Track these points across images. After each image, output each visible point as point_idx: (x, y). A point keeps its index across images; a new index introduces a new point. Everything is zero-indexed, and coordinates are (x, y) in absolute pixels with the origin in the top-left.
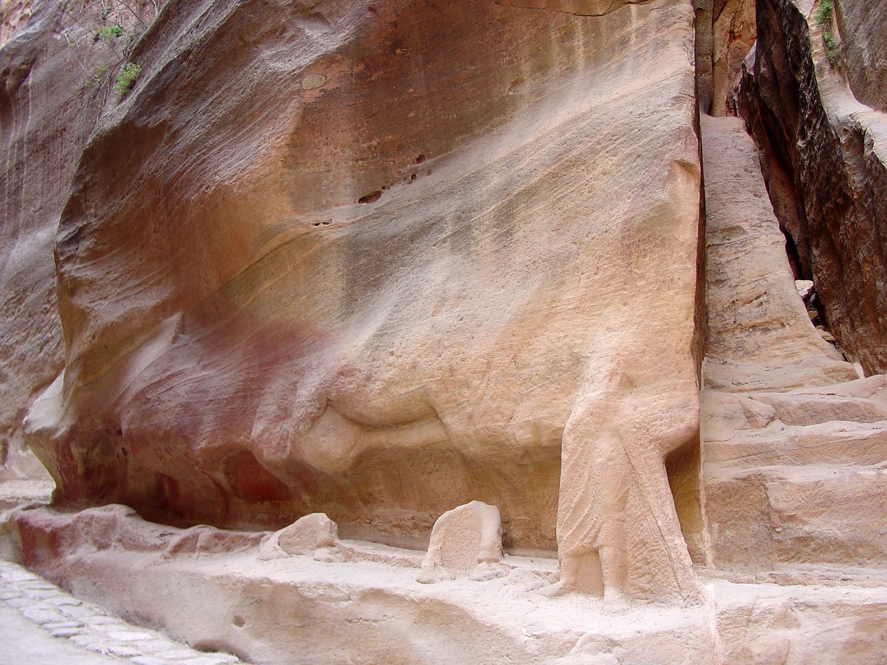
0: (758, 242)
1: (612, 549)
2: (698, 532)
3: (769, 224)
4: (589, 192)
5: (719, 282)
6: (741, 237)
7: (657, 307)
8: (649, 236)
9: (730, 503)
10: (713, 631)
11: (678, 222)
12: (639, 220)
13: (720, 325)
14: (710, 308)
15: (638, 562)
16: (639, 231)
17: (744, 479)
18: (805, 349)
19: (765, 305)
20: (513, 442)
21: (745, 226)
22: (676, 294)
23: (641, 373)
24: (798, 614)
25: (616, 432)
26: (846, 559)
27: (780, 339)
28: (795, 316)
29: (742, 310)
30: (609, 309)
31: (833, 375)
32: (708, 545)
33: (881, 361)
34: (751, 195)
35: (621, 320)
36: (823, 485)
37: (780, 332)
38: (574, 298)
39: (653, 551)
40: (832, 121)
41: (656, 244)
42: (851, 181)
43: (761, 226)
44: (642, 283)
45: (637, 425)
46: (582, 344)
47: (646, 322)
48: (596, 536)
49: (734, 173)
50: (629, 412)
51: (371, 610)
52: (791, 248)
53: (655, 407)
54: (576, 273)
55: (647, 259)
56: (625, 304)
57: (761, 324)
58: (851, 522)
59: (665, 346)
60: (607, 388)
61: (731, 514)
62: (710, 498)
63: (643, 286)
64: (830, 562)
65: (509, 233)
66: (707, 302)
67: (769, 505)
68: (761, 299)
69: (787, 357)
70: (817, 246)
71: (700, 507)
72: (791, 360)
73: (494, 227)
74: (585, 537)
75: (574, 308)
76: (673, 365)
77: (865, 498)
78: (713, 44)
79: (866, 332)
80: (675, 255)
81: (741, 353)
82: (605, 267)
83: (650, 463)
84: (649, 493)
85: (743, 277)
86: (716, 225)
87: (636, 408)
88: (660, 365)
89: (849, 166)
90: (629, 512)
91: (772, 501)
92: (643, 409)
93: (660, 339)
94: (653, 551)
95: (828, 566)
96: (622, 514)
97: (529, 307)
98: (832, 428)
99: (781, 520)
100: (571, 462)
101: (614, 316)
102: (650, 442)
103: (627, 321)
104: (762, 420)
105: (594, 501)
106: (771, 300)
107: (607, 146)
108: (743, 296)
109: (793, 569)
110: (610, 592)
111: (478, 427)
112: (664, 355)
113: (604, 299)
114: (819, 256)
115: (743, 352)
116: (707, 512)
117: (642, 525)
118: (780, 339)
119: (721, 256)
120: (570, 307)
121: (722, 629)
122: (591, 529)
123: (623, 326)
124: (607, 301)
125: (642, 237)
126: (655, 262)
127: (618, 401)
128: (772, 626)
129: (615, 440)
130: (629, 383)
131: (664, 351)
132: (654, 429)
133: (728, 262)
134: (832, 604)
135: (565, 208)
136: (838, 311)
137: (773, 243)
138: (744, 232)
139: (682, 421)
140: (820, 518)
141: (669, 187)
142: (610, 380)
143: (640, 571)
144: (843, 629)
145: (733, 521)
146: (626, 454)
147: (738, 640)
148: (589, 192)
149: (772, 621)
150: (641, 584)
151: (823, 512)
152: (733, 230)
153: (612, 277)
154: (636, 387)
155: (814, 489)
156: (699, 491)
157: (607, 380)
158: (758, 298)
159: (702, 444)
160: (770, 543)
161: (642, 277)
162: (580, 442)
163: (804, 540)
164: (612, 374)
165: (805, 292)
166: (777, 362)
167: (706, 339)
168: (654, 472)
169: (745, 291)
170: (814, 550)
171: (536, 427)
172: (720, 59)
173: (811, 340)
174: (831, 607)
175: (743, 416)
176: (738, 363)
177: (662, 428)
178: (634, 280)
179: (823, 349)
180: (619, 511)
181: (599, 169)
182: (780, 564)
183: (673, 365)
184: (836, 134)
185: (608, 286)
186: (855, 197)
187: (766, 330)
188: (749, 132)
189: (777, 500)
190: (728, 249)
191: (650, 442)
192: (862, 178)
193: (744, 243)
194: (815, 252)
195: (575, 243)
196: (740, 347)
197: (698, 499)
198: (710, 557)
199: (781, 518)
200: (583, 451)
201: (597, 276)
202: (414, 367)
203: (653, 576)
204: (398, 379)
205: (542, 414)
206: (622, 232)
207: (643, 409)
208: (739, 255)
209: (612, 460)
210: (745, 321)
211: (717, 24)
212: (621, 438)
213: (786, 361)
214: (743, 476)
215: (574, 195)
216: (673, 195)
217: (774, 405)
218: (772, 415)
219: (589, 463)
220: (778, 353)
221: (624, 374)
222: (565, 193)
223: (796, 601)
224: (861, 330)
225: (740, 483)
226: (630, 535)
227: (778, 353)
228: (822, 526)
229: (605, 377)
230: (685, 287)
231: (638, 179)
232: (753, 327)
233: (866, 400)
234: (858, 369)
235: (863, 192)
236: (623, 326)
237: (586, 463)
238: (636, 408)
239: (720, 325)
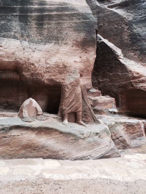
20: (43, 83)
51: (14, 133)
59: (89, 69)
65: (42, 24)
73: (36, 20)
74: (73, 109)
97: (51, 48)
100: (70, 92)
105: (77, 101)
107: (77, 16)
111: (34, 77)
171: (52, 80)
191: (86, 89)
202: (13, 54)
203: (87, 118)
204: (5, 56)
205: (53, 77)
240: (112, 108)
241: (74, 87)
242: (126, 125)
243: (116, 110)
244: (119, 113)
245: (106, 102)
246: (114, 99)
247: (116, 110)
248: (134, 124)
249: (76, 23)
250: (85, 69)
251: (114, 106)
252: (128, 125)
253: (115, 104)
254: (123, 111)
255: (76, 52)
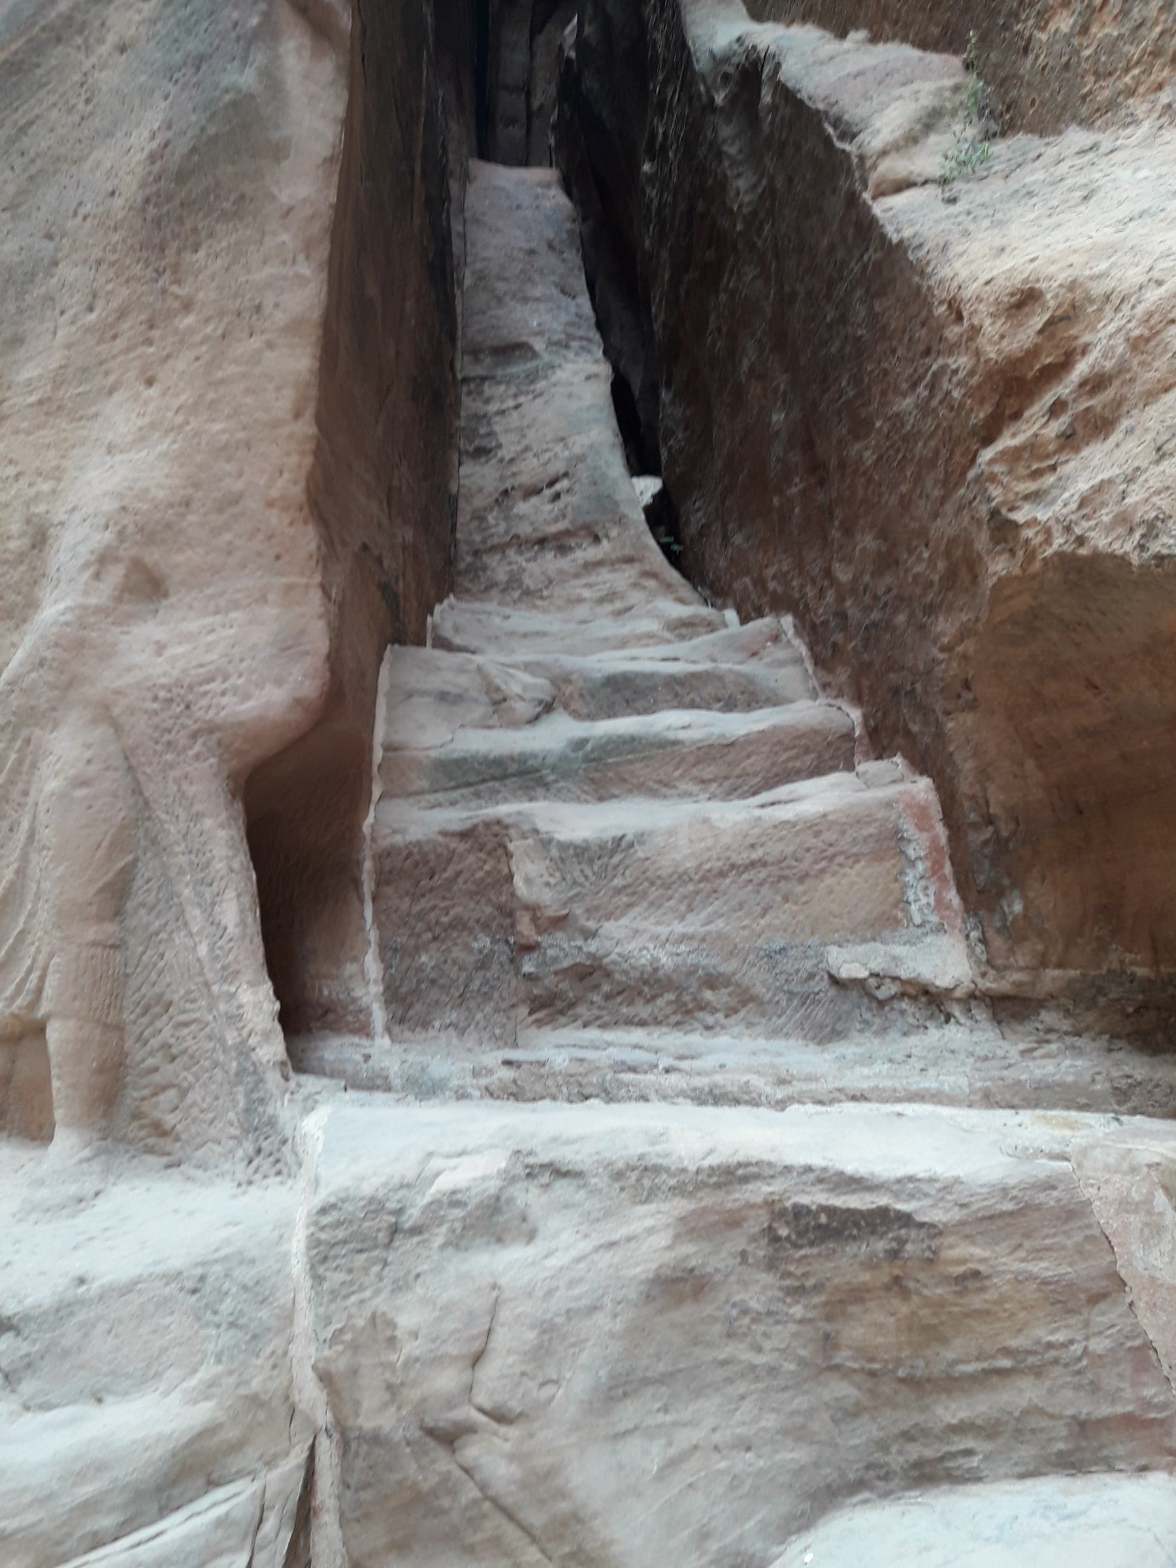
0: (560, 375)
1: (72, 1023)
2: (355, 959)
3: (584, 343)
4: (88, 101)
5: (482, 453)
6: (529, 365)
7: (222, 382)
8: (207, 192)
9: (431, 890)
10: (298, 1266)
11: (278, 152)
12: (182, 146)
13: (477, 538)
14: (462, 504)
15: (151, 1054)
16: (181, 177)
17: (464, 835)
18: (635, 585)
19: (565, 499)
21: (538, 345)
22: (270, 345)
23: (180, 558)
24: (529, 1197)
25: (104, 713)
26: (678, 1017)
27: (590, 566)
28: (621, 521)
29: (522, 507)
30: (117, 397)
31: (683, 628)
32: (376, 989)
33: (774, 594)
34: (555, 292)
35: (140, 422)
36: (631, 845)
37: (591, 553)
38: (41, 377)
39: (186, 1024)
40: (702, 64)
41: (224, 212)
42: (732, 193)
43: (567, 347)
44: (189, 320)
45: (162, 694)
46: (54, 492)
47: (194, 423)
48: (39, 990)
49: (526, 246)
50: (139, 658)
52: (620, 392)
53: (209, 648)
54: (49, 313)
55: (202, 253)
56: (150, 382)
57: (558, 536)
58: (690, 930)
59: (239, 486)
60: (86, 593)
61: (432, 916)
62: (383, 878)
63: (191, 331)
64: (642, 1024)
66: (454, 489)
67: (513, 895)
68: (558, 487)
69: (601, 601)
70: (668, 386)
71: (361, 900)
72: (608, 608)
75: (40, 402)
76: (261, 536)
77: (722, 874)
78: (530, 71)
79: (747, 538)
80: (269, 242)
81: (516, 594)
82: (110, 287)
83: (191, 790)
84: (182, 871)
85: (525, 442)
86: (479, 338)
87: (164, 649)
88: (227, 537)
89: (729, 156)
90: (132, 922)
91: (518, 882)
92: (180, 650)
93: (228, 467)
94: (186, 1024)
95: (638, 1035)
96: (110, 927)
98: (669, 721)
99: (537, 926)
101: (121, 417)
102: (194, 736)
103: (153, 426)
104: (523, 709)
106: (577, 487)
108: (524, 479)
109: (557, 1047)
110: (66, 1144)
112: (236, 510)
113: (107, 374)
114: (672, 403)
115: (520, 592)
116: (376, 914)
117: (162, 956)
118: (590, 566)
119: (487, 401)
120: (32, 399)
121: (321, 1255)
122: (29, 971)
123: (141, 438)
124: (112, 378)
125: (193, 194)
126: (219, 262)
127: (116, 630)
128: (457, 1242)
129: (102, 732)
130: (147, 587)
131: (235, 499)
132: (204, 702)
133: (502, 412)
134: (620, 1165)
135: (32, 153)
136: (700, 514)
137: (588, 378)
138: (535, 355)
139: (279, 682)
140: (624, 921)
141: (259, 58)
142: (97, 576)
143: (156, 1078)
144: (649, 1237)
145: (437, 931)
146: (130, 769)
147: (362, 1288)
148: (88, 101)
149: (458, 1225)
150: (156, 1114)
151: (630, 906)
152: (512, 350)
153: (122, 314)
154: (166, 595)
155: (613, 853)
156: (359, 864)
157: (86, 575)
158: (551, 484)
159: (378, 755)
160: (514, 983)
161: (187, 306)
162: (13, 740)
163: (589, 973)
164: (103, 559)
165: (647, 499)
166: (582, 611)
167: (451, 562)
168: (199, 816)
169: (529, 470)
170: (608, 997)
172: (541, 106)
173: (648, 568)
174: (618, 1175)
175: (484, 698)
176: (507, 611)
177: (224, 700)
178: (170, 315)
179: (669, 587)
180: (100, 919)
181: (112, 39)
182: (533, 1031)
183: (261, 536)
184: (708, 90)
185: (115, 337)
186: (739, 227)
187: (563, 550)
188: (569, 193)
189: (528, 881)
190: (502, 388)
191: (194, 736)
192: (754, 180)
193: (532, 377)
194: (665, 396)
195: (49, 237)
196: (514, 581)
197: (357, 883)
198: (379, 1016)
199: (535, 920)
200: (20, 762)
201: (93, 316)
203: (184, 1093)
206: (143, 186)
207: (180, 650)
208: (522, 399)
209: (85, 783)
210: (524, 529)
211: (541, 39)
212: (117, 727)
213: (599, 610)
214: (457, 827)
215: (55, 113)
216: (271, 79)
217: (553, 682)
218: (548, 699)
219: (33, 793)
220: (586, 593)
221: (137, 565)
222: (37, 111)
223: (531, 1160)
224: (738, 539)
225: (454, 844)
226: (133, 983)
227: (586, 593)
228: (638, 939)
229: (86, 566)
230: (293, 327)
231: (192, 45)
232: (542, 542)
233: (737, 667)
234: (731, 615)
235: (754, 213)
236: (141, 438)
237: (25, 793)
238: (164, 649)
239: (477, 538)
240: (887, 920)
241: (25, 732)
242: (757, 1222)
243: (946, 961)
244: (1006, 1008)
245: (774, 850)
246: (922, 788)
247: (946, 961)
248: (937, 1216)
249: (122, 49)
250: (187, 503)
251: (925, 893)
252: (799, 1212)
253: (936, 869)
254: (1043, 962)
255: (120, 343)
